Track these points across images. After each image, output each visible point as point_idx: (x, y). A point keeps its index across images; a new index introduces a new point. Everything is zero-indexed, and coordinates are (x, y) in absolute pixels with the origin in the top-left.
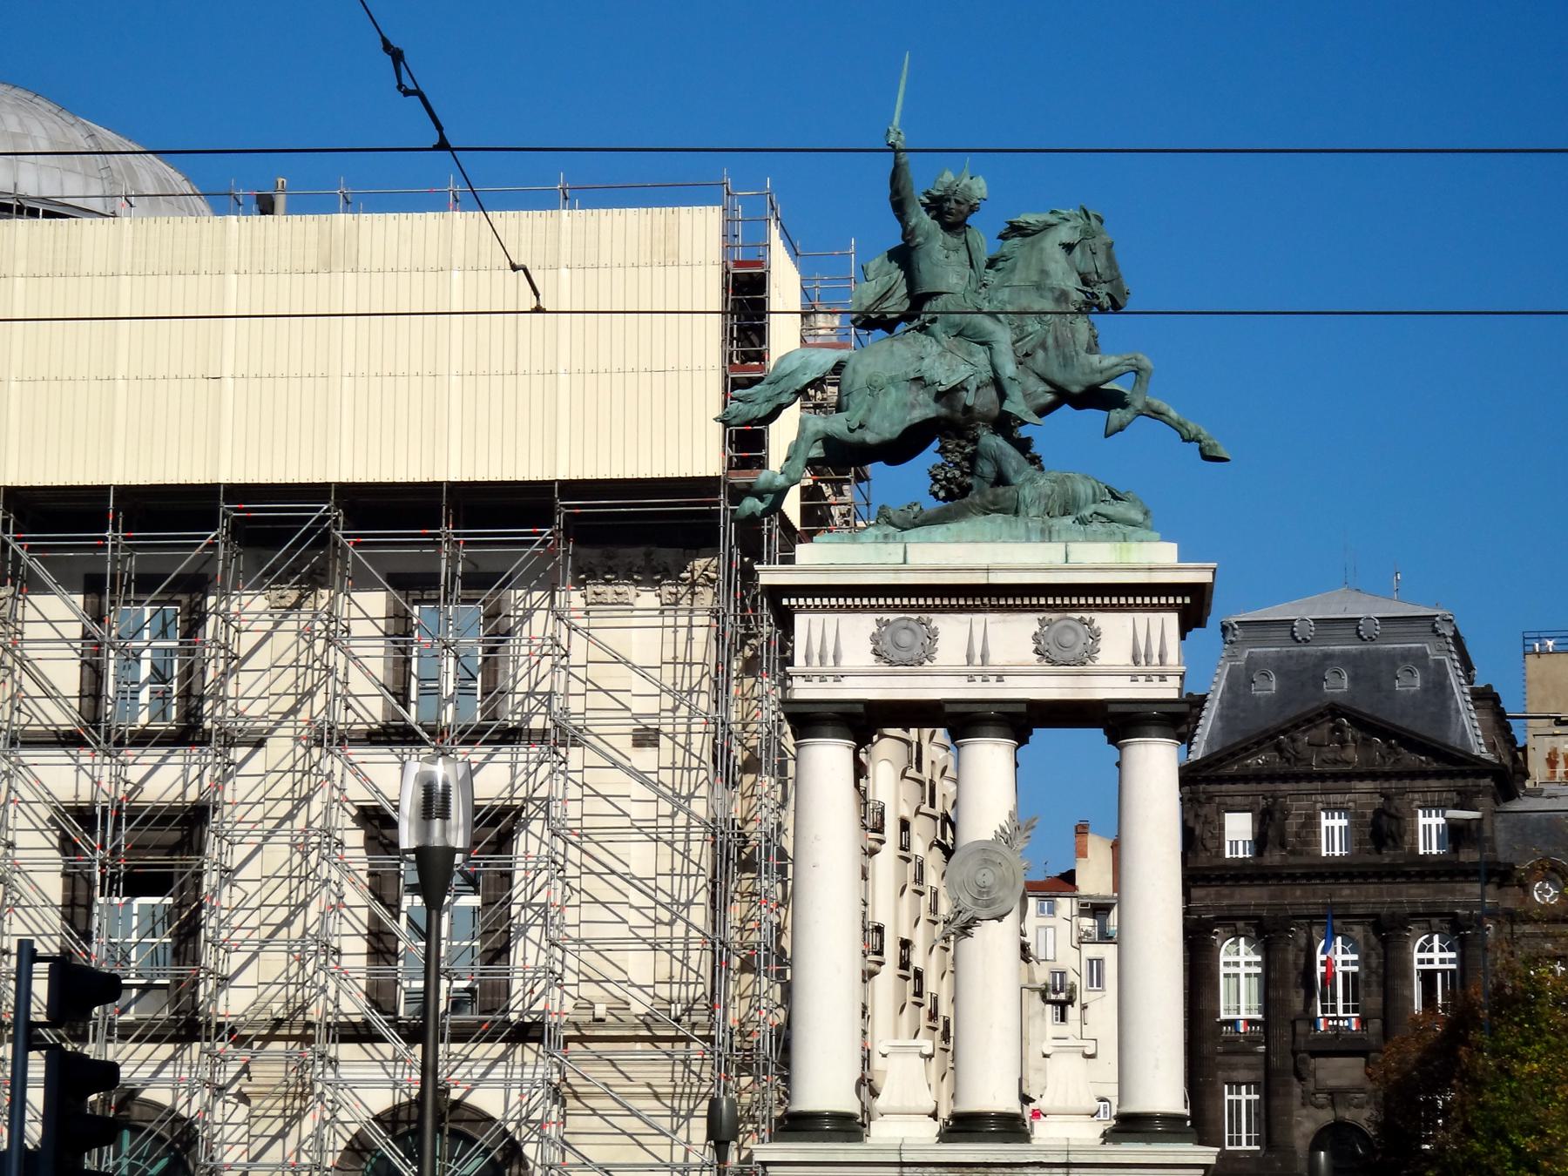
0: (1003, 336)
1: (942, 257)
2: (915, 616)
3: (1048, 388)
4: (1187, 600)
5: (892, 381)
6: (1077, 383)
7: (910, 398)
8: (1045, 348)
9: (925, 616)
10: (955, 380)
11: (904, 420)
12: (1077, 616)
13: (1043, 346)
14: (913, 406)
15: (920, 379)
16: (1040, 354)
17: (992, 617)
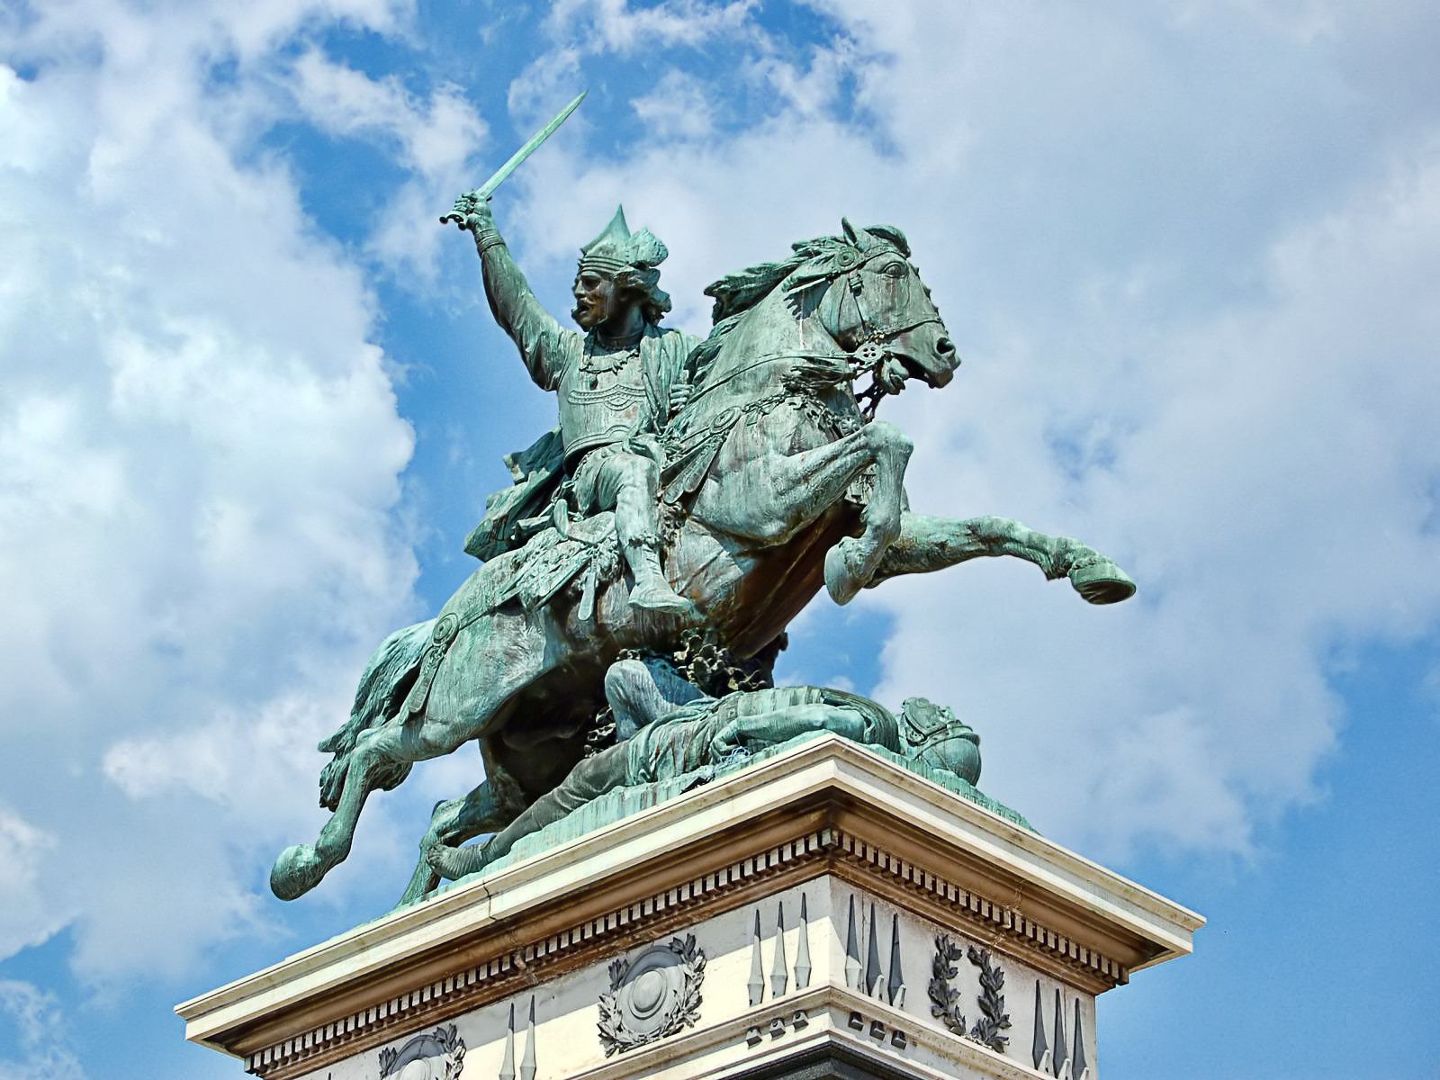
0: (633, 475)
1: (584, 388)
2: (431, 1031)
3: (737, 549)
4: (826, 840)
5: (469, 622)
6: (769, 516)
7: (500, 644)
8: (718, 477)
9: (445, 1025)
10: (559, 579)
11: (489, 684)
12: (667, 941)
13: (714, 472)
14: (512, 657)
15: (512, 606)
16: (711, 486)
17: (540, 993)
